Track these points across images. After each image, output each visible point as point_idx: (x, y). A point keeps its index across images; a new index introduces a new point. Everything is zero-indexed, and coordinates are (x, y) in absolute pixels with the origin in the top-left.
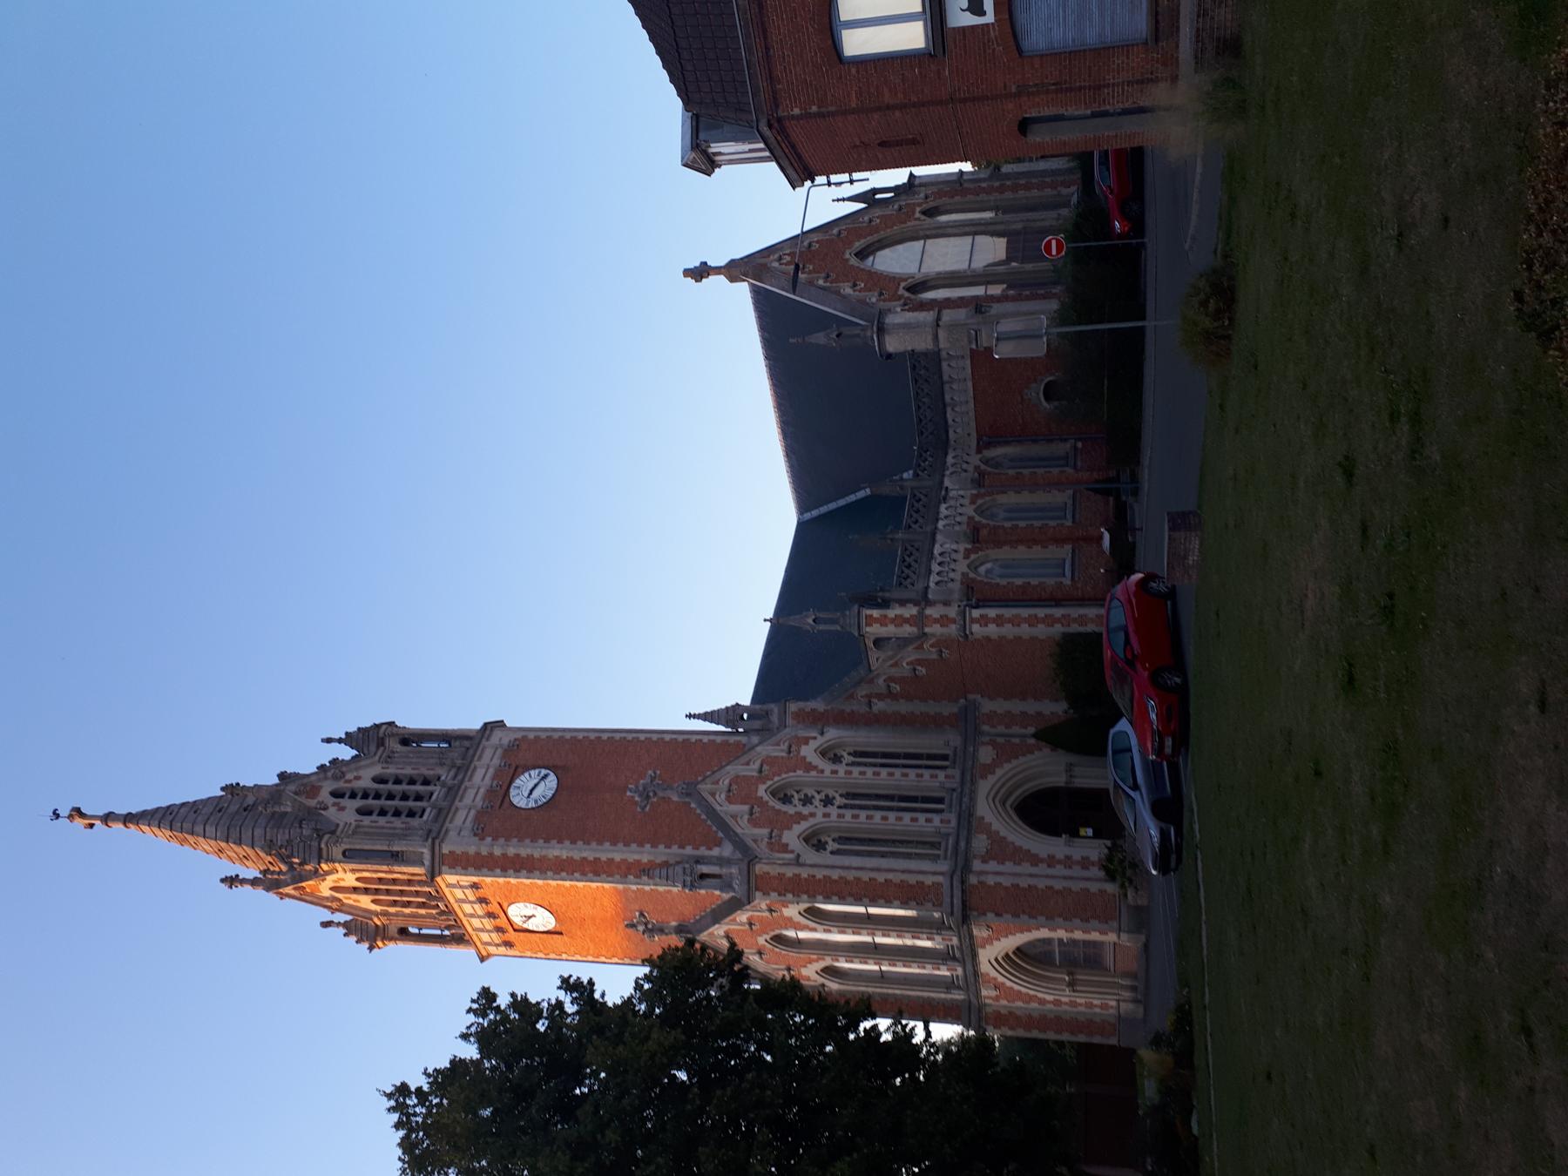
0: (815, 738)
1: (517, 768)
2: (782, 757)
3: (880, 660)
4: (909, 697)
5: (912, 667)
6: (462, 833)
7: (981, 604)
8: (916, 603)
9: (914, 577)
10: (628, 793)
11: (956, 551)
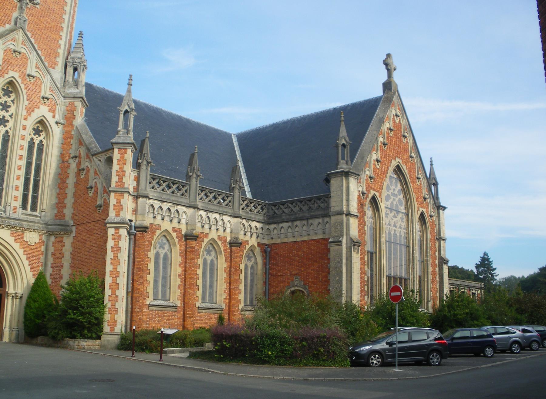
0: (54, 117)
2: (40, 92)
3: (99, 162)
4: (77, 185)
5: (93, 186)
7: (132, 237)
8: (137, 189)
9: (159, 190)
11: (179, 222)
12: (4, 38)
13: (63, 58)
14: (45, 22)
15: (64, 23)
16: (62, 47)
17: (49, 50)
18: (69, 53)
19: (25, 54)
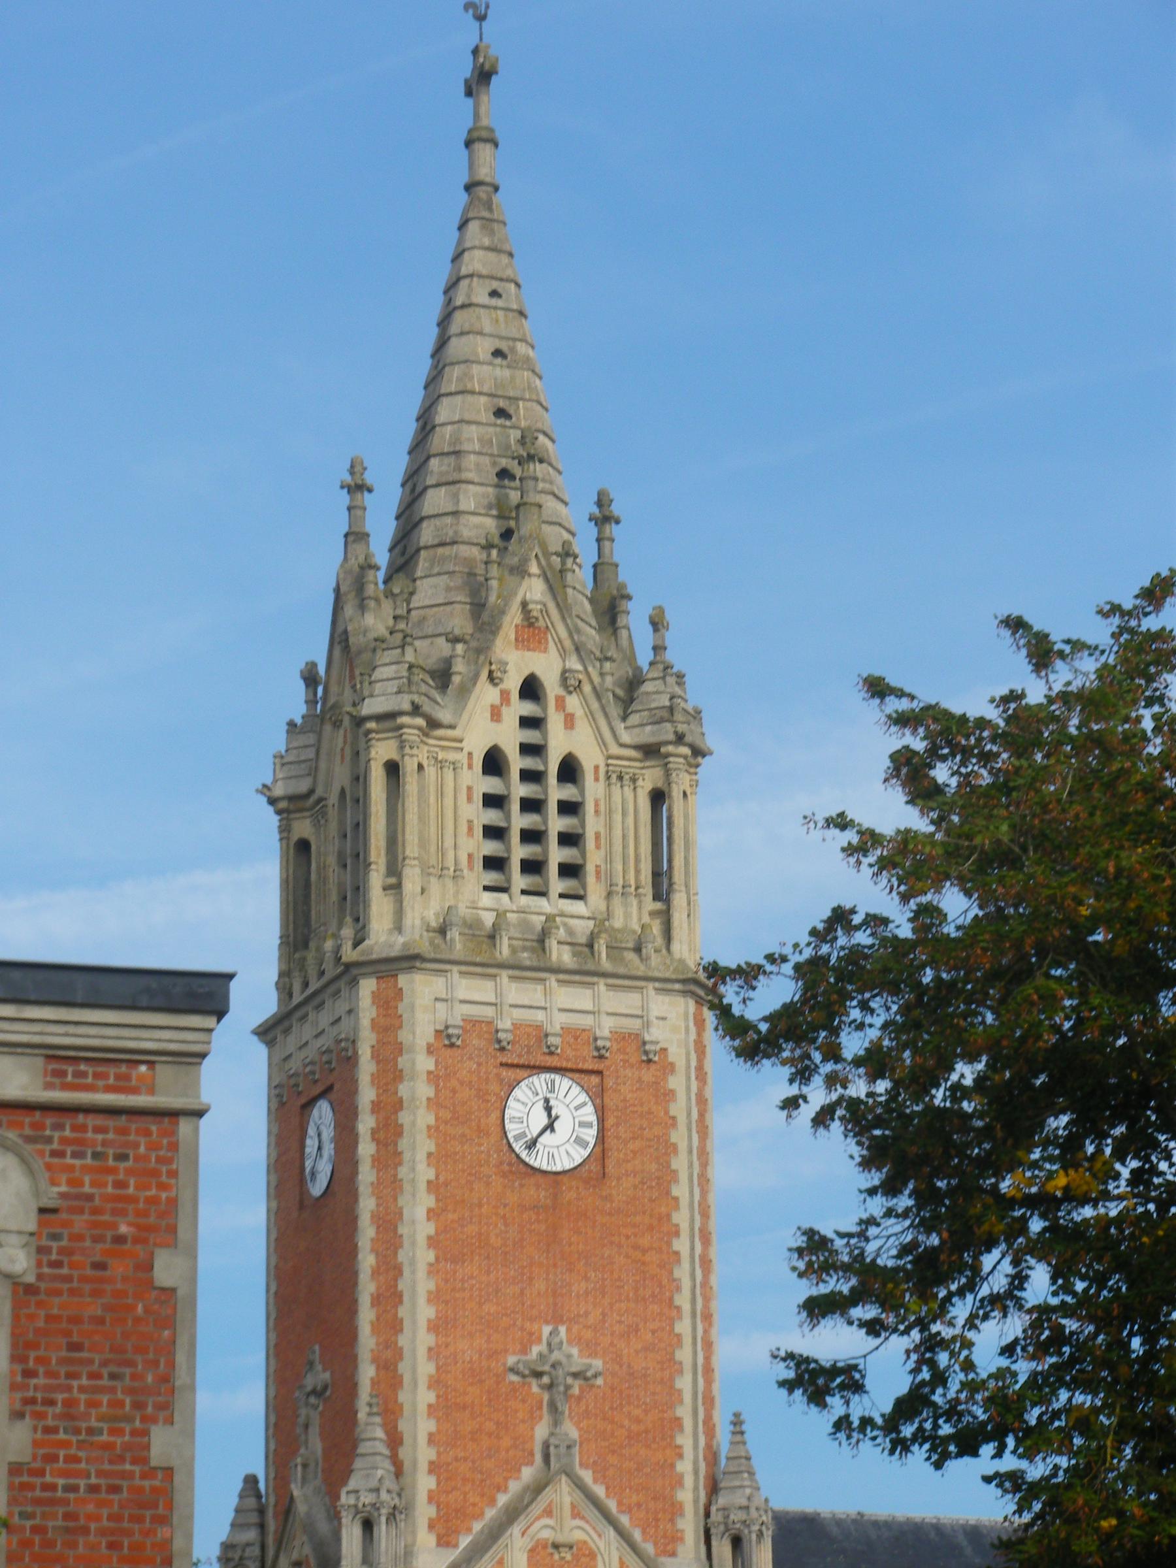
1: (599, 1073)
6: (439, 1005)
10: (547, 1330)
12: (522, 1517)
13: (696, 1513)
14: (626, 1423)
15: (681, 1402)
16: (689, 1481)
17: (652, 1505)
18: (714, 1489)
19: (585, 1542)
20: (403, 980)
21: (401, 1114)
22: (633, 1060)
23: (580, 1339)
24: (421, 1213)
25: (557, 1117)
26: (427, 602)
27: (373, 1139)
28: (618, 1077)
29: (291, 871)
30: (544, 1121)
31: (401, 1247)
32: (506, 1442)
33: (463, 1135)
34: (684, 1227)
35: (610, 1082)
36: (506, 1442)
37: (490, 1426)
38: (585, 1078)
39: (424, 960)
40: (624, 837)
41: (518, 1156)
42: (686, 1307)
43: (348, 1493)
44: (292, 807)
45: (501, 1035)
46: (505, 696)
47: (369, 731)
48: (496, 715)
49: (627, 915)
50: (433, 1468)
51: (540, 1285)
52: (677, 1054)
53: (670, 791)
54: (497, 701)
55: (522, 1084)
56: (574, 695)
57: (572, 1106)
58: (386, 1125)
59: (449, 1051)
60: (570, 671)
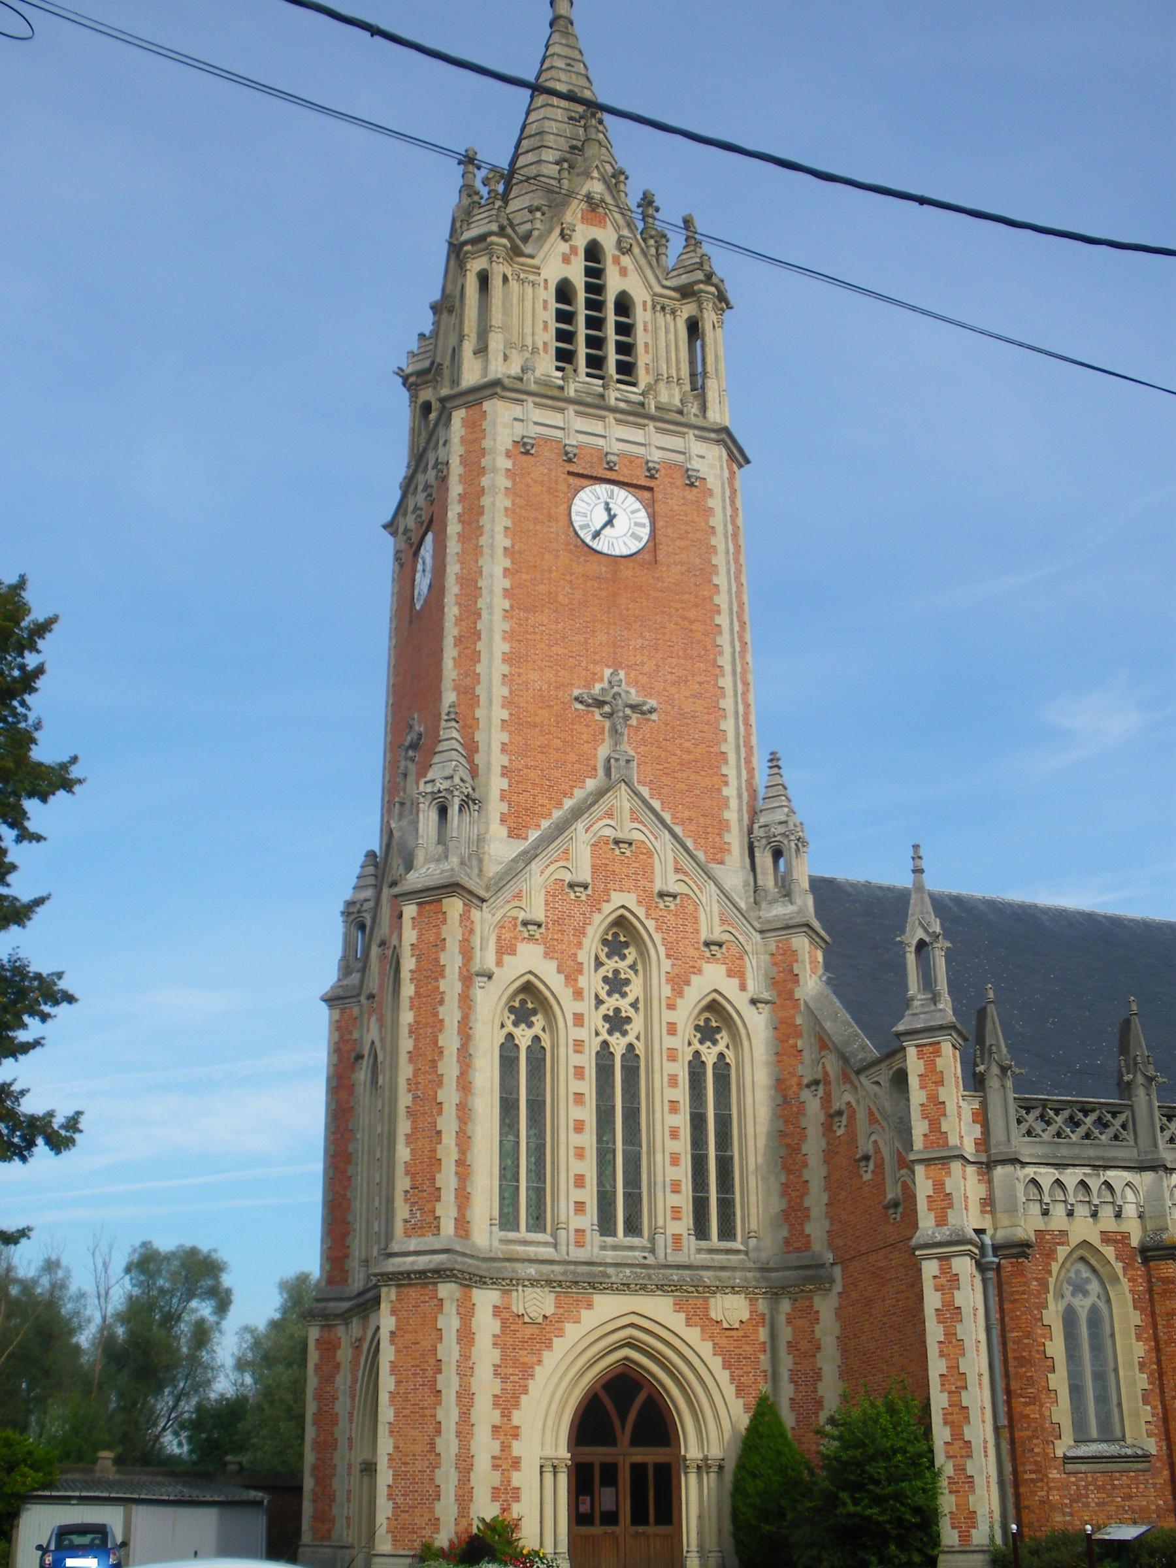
0: (743, 988)
1: (650, 489)
2: (697, 931)
3: (876, 1088)
4: (829, 1155)
5: (871, 1153)
6: (516, 424)
7: (991, 1274)
8: (984, 1143)
9: (1046, 1136)
10: (608, 672)
11: (1118, 1215)
12: (586, 815)
13: (741, 830)
14: (678, 752)
15: (726, 740)
16: (734, 803)
17: (702, 820)
18: (754, 813)
19: (643, 842)
20: (487, 405)
21: (482, 499)
22: (679, 483)
23: (637, 683)
24: (498, 571)
25: (615, 516)
26: (516, 209)
27: (460, 521)
28: (665, 494)
29: (417, 422)
30: (605, 518)
31: (481, 596)
32: (572, 757)
33: (536, 518)
34: (724, 607)
35: (659, 496)
36: (572, 757)
37: (557, 743)
38: (640, 493)
39: (505, 388)
40: (667, 346)
41: (583, 542)
42: (728, 668)
43: (426, 783)
44: (419, 381)
45: (569, 449)
46: (574, 250)
47: (467, 253)
48: (566, 260)
49: (671, 396)
50: (505, 772)
51: (602, 637)
52: (713, 482)
53: (702, 317)
54: (568, 251)
55: (586, 489)
56: (627, 256)
57: (628, 510)
58: (471, 509)
59: (525, 458)
60: (623, 237)
